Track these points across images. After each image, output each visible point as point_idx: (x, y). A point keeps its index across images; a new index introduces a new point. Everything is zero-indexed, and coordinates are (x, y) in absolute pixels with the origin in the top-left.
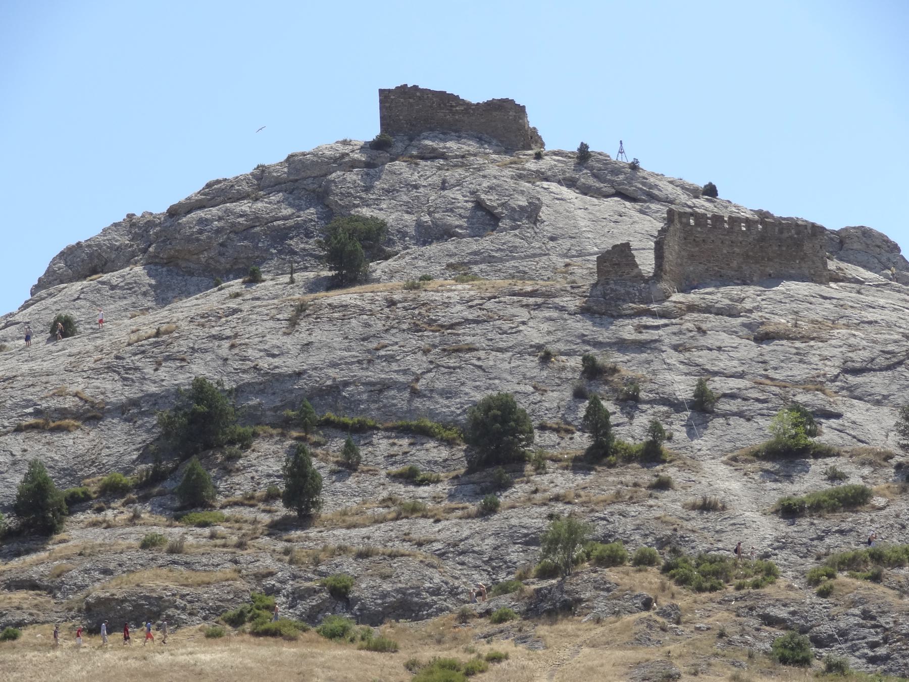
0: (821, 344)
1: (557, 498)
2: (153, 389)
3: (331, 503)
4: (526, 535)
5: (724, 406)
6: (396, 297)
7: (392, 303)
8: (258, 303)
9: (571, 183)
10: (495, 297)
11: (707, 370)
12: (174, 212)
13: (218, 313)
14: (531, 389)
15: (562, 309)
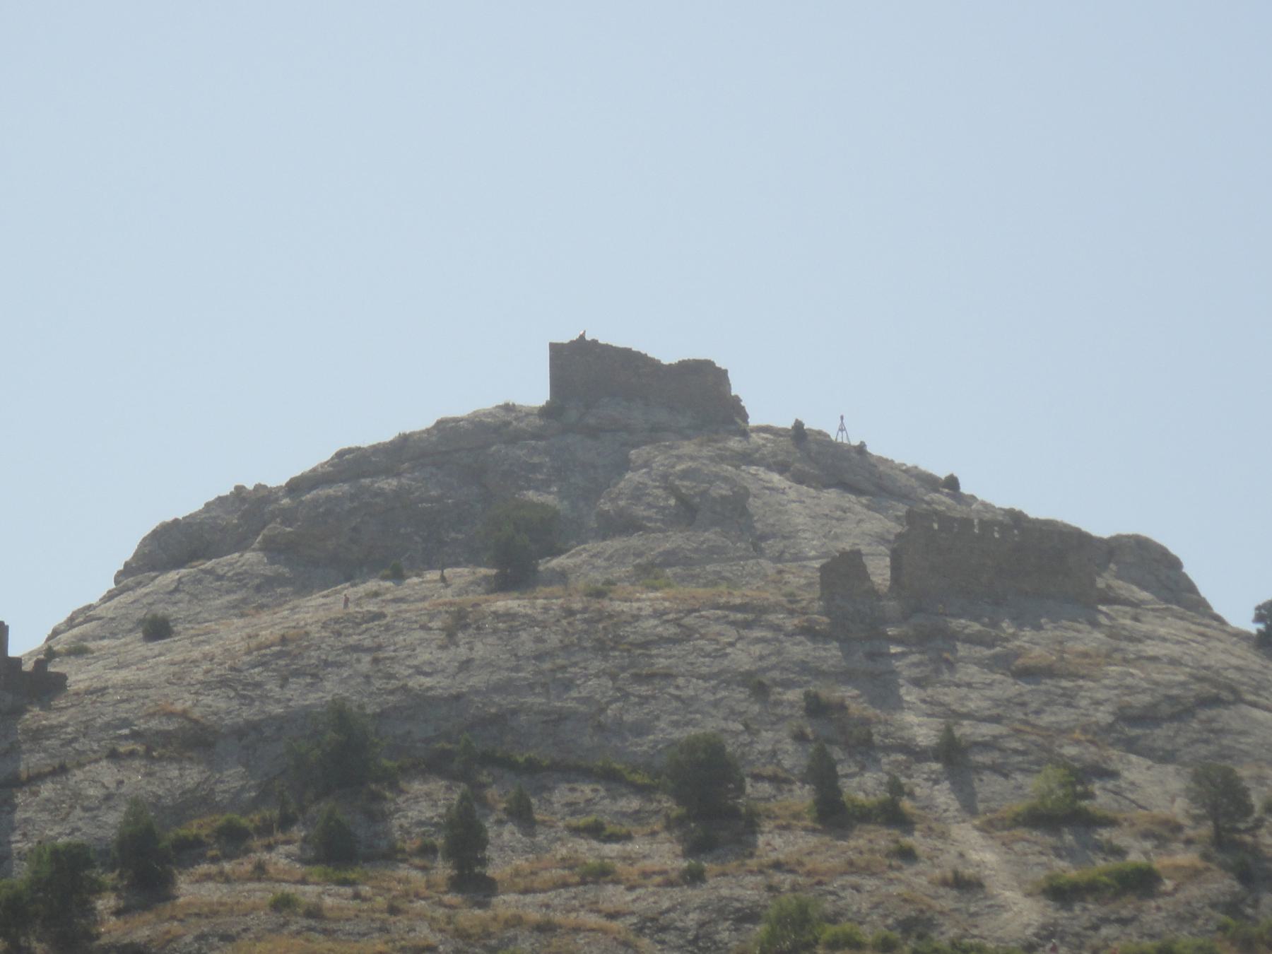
0: (1091, 684)
1: (778, 866)
2: (278, 710)
3: (498, 861)
4: (738, 910)
5: (980, 758)
6: (577, 606)
7: (570, 613)
8: (404, 606)
9: (782, 468)
10: (695, 611)
11: (954, 712)
12: (296, 486)
13: (356, 618)
14: (741, 727)
15: (777, 628)
